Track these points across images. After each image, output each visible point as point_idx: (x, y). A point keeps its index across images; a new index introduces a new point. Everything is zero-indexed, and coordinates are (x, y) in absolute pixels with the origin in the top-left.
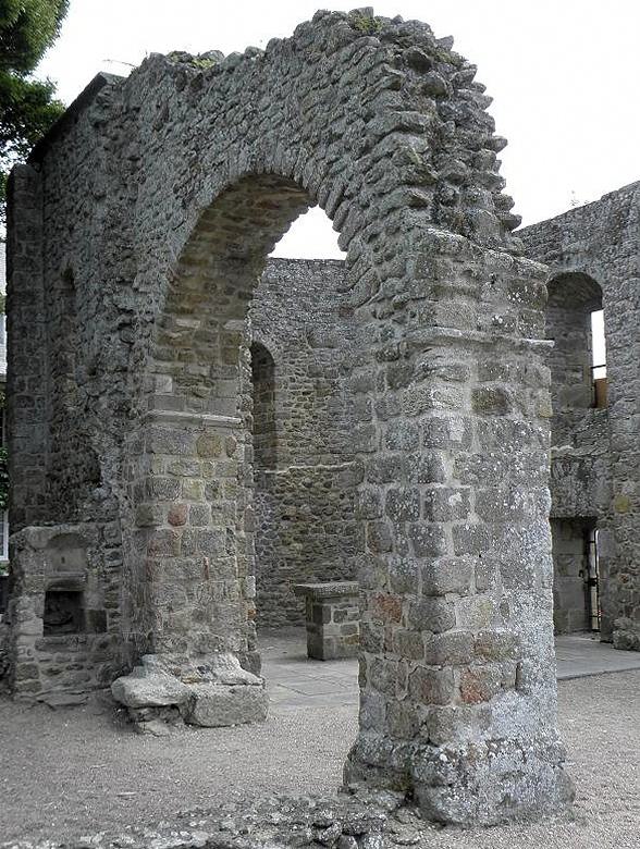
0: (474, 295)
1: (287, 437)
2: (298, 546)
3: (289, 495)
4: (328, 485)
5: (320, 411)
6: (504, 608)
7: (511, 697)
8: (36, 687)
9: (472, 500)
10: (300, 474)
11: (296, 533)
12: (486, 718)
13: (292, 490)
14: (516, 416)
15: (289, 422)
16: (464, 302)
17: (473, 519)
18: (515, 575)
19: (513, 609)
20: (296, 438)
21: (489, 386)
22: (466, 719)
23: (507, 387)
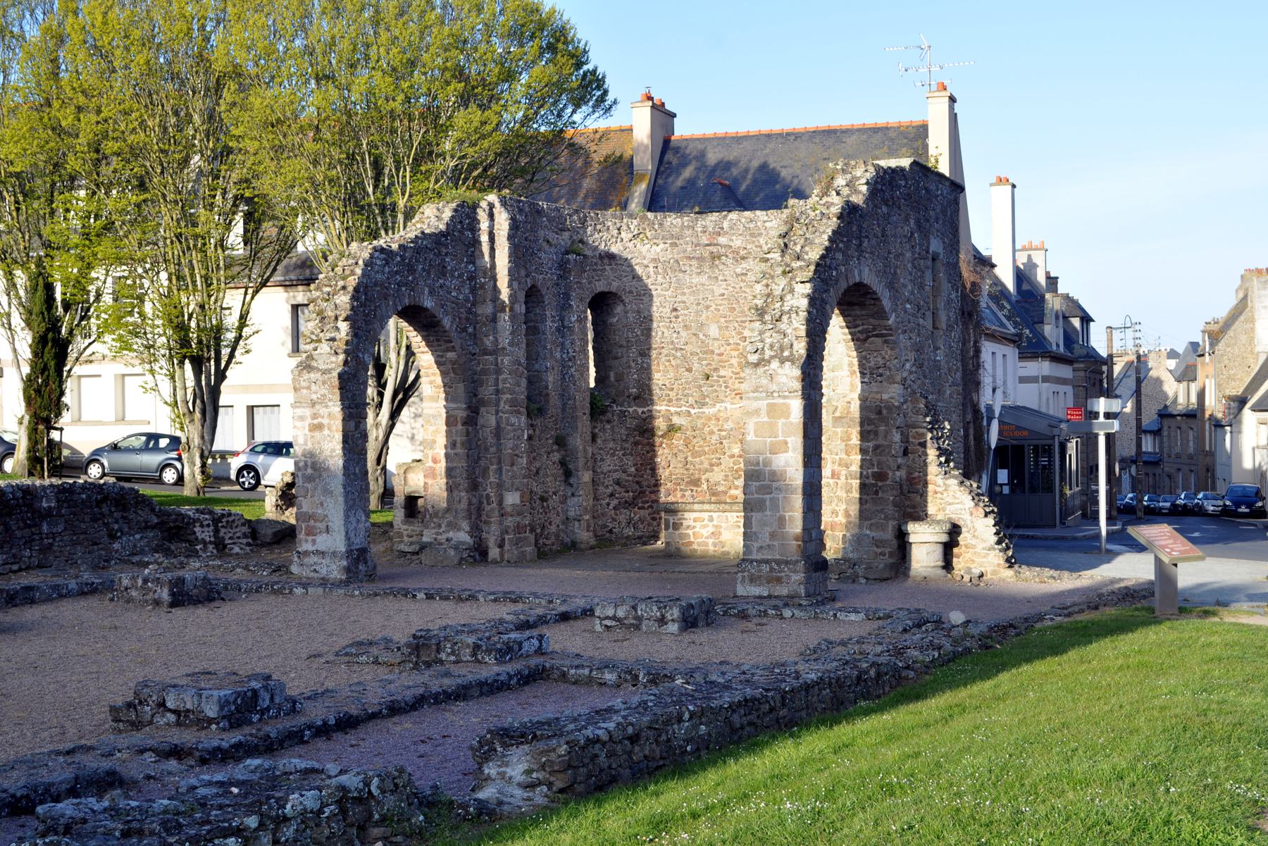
0: (309, 388)
6: (322, 504)
12: (314, 542)
14: (326, 432)
16: (305, 391)
18: (327, 492)
21: (315, 422)
22: (306, 541)
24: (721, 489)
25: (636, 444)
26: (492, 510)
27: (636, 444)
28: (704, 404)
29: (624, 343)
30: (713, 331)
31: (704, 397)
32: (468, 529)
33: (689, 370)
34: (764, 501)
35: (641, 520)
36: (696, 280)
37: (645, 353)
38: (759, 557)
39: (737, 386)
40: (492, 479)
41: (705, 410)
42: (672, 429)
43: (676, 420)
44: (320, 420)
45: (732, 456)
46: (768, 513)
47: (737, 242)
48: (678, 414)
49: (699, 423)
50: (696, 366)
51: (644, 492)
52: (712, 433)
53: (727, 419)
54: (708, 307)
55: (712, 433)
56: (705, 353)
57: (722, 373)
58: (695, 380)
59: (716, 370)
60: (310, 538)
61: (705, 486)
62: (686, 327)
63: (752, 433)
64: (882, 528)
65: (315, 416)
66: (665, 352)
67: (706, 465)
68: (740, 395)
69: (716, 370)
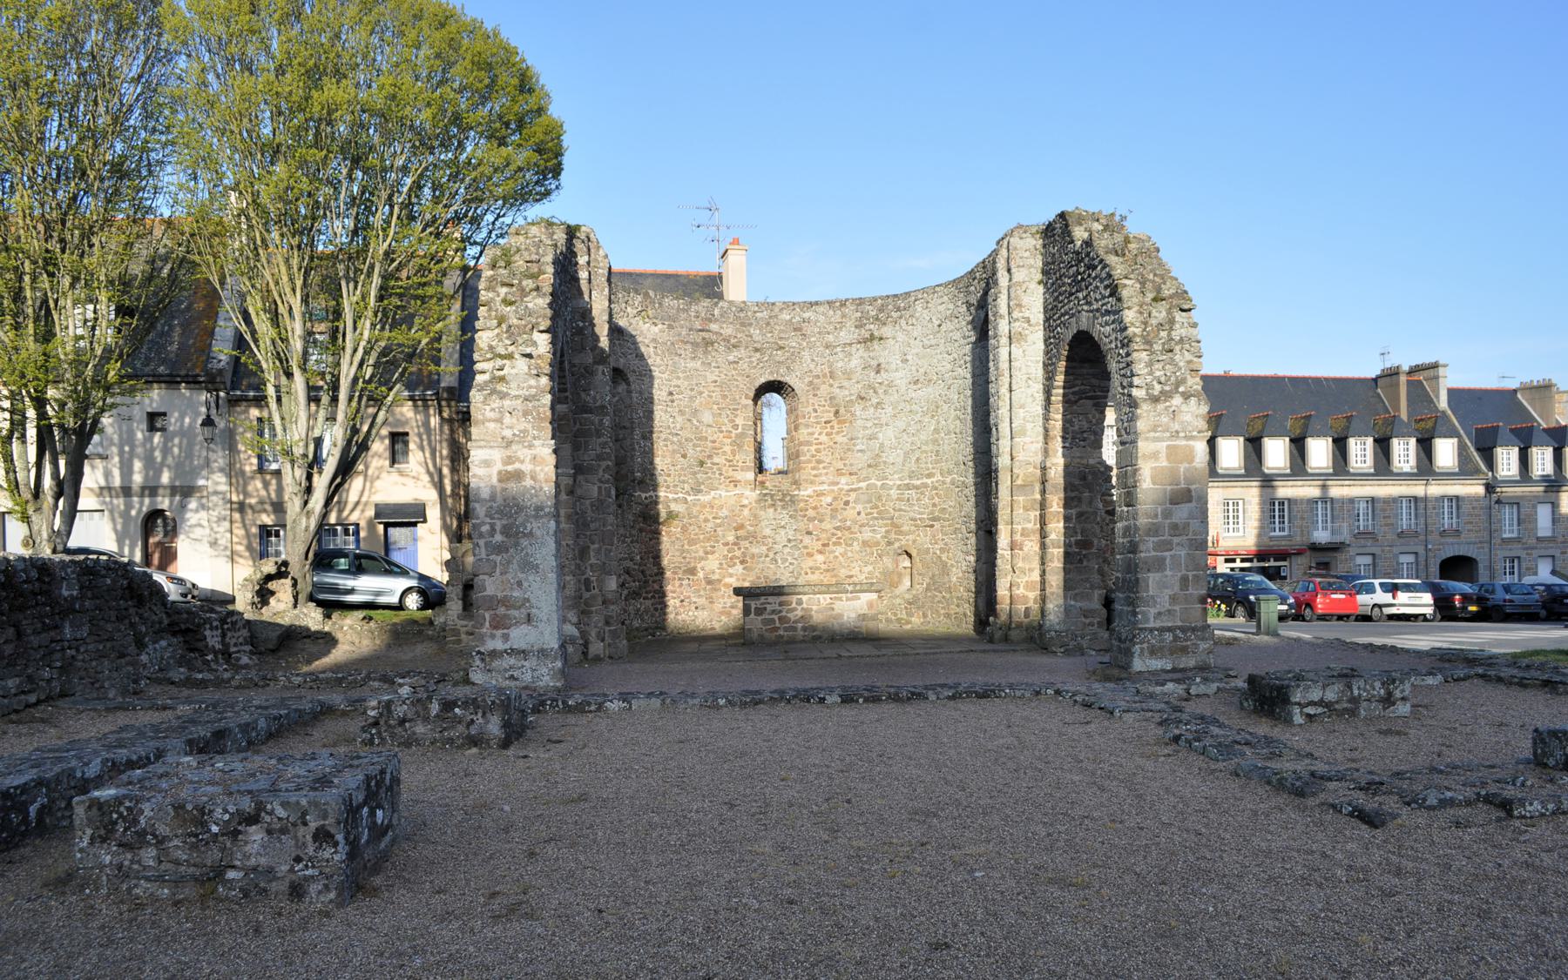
0: (499, 421)
1: (809, 461)
2: (820, 558)
3: (811, 513)
4: (847, 503)
5: (839, 439)
6: (520, 584)
7: (524, 628)
8: (459, 642)
9: (498, 528)
10: (820, 494)
11: (818, 545)
12: (506, 638)
13: (815, 508)
15: (813, 448)
16: (492, 425)
17: (498, 538)
18: (528, 566)
19: (525, 584)
20: (819, 462)
21: (510, 468)
22: (493, 637)
23: (523, 467)
24: (716, 577)
25: (641, 530)
26: (594, 597)
27: (641, 530)
28: (700, 491)
29: (628, 425)
30: (707, 417)
31: (699, 484)
32: (575, 620)
33: (684, 456)
34: (1164, 559)
35: (646, 611)
36: (691, 365)
37: (648, 435)
38: (1158, 624)
39: (731, 473)
40: (593, 561)
41: (699, 497)
42: (672, 516)
43: (673, 507)
44: (517, 466)
45: (726, 544)
46: (1168, 573)
47: (728, 330)
48: (675, 500)
49: (695, 511)
50: (690, 452)
51: (646, 582)
52: (706, 520)
53: (721, 507)
54: (701, 393)
55: (706, 520)
56: (700, 439)
57: (716, 460)
58: (690, 467)
59: (710, 457)
60: (499, 633)
61: (701, 575)
62: (681, 412)
63: (1148, 480)
64: (1088, 597)
65: (509, 460)
66: (663, 436)
67: (701, 553)
68: (735, 483)
69: (710, 457)
